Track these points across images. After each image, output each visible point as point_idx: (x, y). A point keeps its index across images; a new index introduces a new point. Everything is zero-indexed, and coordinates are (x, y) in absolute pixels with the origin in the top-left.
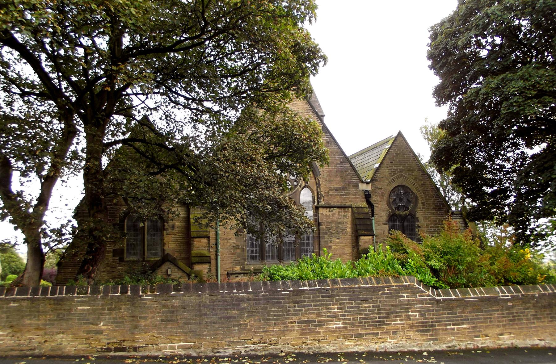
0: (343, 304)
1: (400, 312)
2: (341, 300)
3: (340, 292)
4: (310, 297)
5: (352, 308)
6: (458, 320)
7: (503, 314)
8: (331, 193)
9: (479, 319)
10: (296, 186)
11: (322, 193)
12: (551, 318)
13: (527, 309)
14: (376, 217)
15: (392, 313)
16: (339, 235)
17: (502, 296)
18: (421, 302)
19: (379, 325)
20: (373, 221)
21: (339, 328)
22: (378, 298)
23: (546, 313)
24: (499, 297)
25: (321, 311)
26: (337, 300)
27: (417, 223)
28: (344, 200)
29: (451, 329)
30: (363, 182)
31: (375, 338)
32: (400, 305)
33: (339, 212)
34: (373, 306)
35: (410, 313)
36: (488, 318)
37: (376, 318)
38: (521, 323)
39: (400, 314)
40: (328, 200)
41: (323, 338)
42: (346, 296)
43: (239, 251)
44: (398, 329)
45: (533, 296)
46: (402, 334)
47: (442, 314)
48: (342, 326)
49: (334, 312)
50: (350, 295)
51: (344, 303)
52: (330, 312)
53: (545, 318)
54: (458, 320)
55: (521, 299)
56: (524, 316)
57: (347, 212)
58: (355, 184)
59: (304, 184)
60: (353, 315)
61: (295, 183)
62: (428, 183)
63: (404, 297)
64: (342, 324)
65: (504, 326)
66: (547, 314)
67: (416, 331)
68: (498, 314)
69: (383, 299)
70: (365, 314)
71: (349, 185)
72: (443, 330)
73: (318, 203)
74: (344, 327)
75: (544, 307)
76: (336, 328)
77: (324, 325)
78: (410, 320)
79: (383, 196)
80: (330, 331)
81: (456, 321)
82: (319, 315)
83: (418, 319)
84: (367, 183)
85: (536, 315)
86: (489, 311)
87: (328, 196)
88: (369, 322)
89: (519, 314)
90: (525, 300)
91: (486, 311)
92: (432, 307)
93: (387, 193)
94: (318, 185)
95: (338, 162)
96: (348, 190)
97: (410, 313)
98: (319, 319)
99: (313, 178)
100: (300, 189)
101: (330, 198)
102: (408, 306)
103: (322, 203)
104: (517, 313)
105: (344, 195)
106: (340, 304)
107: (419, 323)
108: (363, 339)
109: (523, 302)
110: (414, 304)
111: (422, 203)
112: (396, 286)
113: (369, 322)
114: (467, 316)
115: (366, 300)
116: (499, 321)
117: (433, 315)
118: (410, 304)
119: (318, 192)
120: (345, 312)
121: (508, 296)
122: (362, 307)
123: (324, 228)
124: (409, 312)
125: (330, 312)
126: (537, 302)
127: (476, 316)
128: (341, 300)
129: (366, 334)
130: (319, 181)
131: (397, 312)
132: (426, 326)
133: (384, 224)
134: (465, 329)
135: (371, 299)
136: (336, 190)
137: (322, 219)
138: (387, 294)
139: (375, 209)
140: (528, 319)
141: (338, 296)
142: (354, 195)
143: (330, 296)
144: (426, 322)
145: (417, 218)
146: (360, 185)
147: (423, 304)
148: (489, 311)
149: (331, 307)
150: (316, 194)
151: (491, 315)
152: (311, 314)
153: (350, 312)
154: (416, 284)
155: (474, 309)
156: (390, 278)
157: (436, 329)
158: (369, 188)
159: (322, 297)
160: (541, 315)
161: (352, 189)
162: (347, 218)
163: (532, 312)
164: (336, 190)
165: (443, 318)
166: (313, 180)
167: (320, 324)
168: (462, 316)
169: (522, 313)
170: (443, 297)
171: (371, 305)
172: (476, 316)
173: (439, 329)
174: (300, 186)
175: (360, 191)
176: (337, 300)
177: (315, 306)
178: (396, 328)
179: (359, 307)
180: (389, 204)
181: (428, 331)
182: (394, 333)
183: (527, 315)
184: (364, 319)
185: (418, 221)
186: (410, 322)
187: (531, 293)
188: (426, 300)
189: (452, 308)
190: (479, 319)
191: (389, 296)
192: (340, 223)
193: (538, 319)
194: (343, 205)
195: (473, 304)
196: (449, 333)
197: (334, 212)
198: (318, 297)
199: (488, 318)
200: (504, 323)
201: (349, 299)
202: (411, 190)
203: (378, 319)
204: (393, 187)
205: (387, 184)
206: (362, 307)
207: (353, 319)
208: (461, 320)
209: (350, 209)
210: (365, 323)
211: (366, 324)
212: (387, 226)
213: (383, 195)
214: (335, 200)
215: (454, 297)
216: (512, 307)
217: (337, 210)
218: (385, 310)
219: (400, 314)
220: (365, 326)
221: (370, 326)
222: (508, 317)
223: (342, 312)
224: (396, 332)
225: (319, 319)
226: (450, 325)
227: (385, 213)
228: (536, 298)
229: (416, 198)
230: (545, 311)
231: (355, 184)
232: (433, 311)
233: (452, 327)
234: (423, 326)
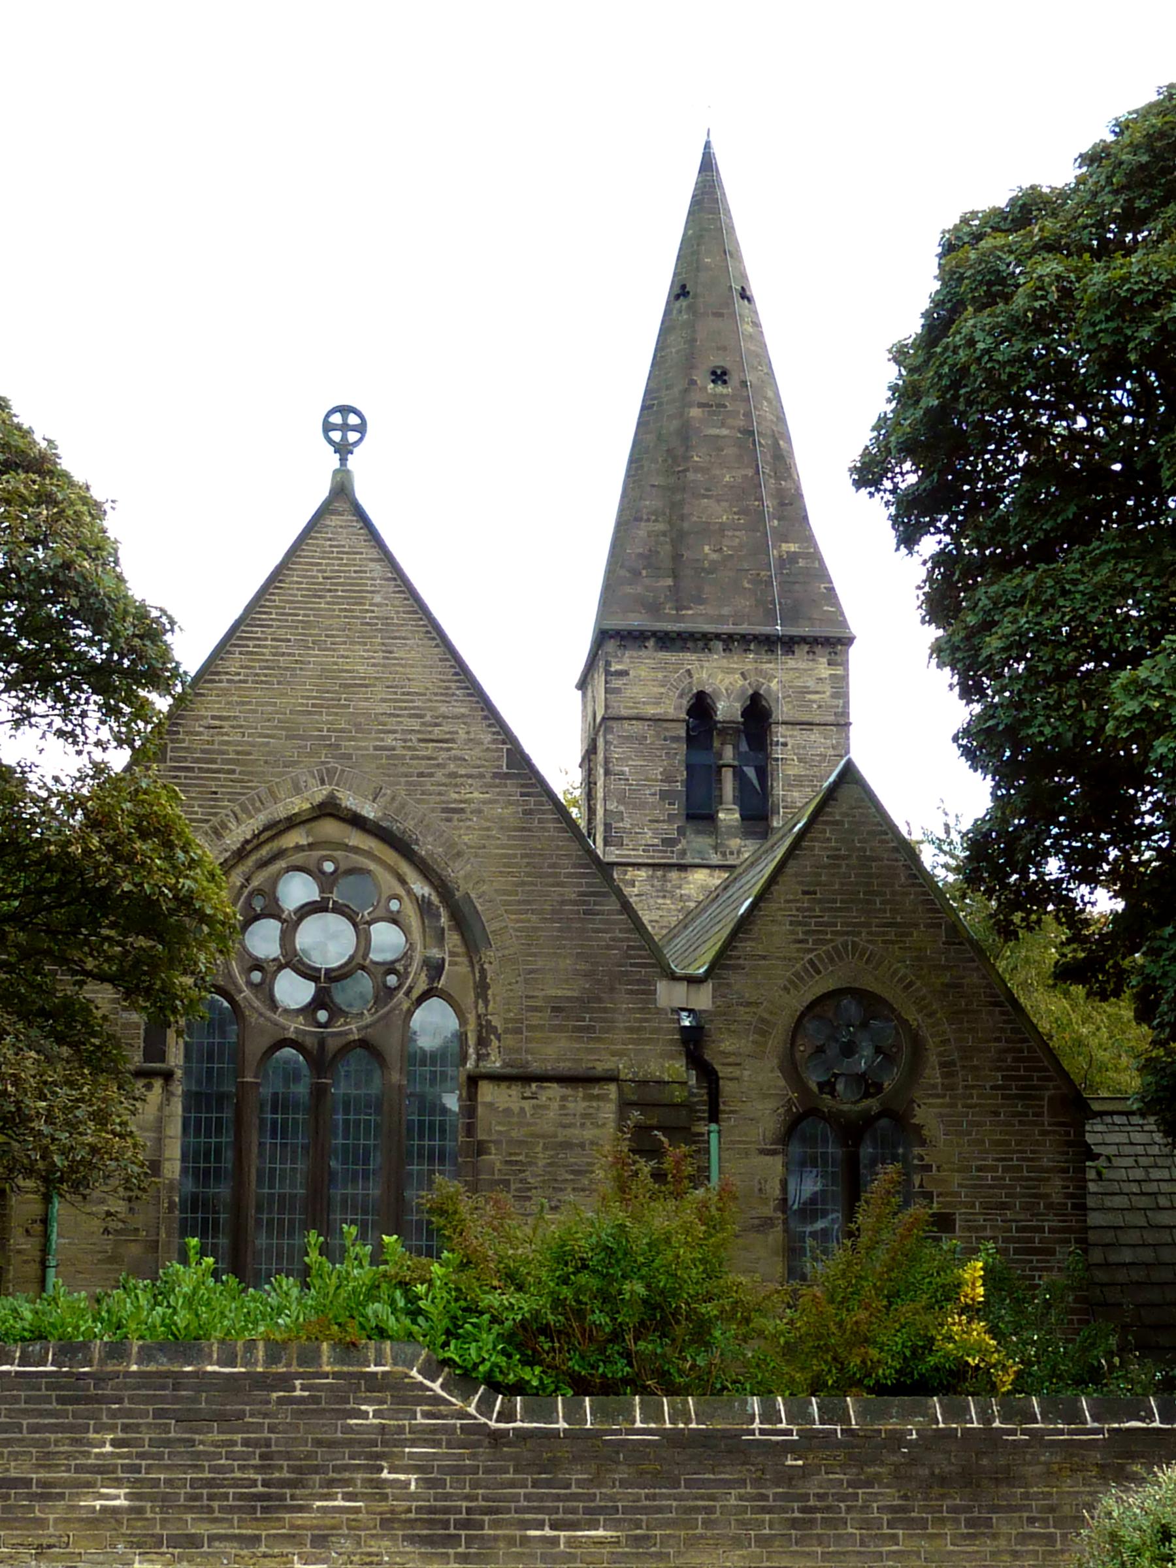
0: (136, 1428)
1: (346, 1468)
2: (129, 1413)
3: (126, 1387)
4: (16, 1399)
5: (168, 1443)
6: (574, 1511)
7: (764, 1497)
8: (535, 1019)
9: (659, 1510)
10: (391, 992)
11: (496, 1022)
12: (970, 1523)
13: (869, 1483)
14: (729, 1122)
15: (316, 1470)
16: (560, 1196)
17: (762, 1432)
18: (428, 1436)
19: (265, 1509)
20: (714, 1137)
21: (115, 1510)
22: (266, 1415)
23: (947, 1503)
24: (752, 1432)
25: (53, 1449)
26: (113, 1415)
27: (917, 1150)
28: (590, 1051)
29: (543, 1539)
30: (674, 977)
31: (244, 1552)
32: (349, 1443)
33: (564, 1098)
34: (246, 1443)
35: (385, 1475)
36: (697, 1510)
37: (254, 1483)
38: (839, 1537)
39: (347, 1475)
40: (518, 1051)
41: (52, 1541)
42: (148, 1400)
43: (135, 1250)
44: (333, 1528)
45: (897, 1439)
46: (349, 1545)
47: (512, 1484)
48: (126, 1503)
49: (98, 1456)
50: (163, 1399)
51: (138, 1425)
52: (87, 1455)
53: (942, 1521)
54: (574, 1511)
55: (840, 1445)
56: (849, 1509)
57: (598, 1098)
58: (639, 982)
59: (422, 986)
60: (168, 1468)
61: (392, 980)
62: (975, 978)
63: (364, 1415)
64: (127, 1497)
65: (762, 1541)
66: (954, 1509)
67: (405, 1538)
68: (741, 1498)
69: (285, 1417)
70: (212, 1469)
71: (612, 990)
72: (511, 1541)
73: (480, 1057)
74: (131, 1510)
75: (943, 1481)
76: (104, 1509)
77: (61, 1496)
78: (384, 1497)
79: (763, 1033)
80: (81, 1520)
81: (567, 1511)
82: (46, 1460)
83: (413, 1497)
84: (692, 980)
85: (903, 1509)
86: (703, 1484)
87: (518, 1031)
88: (225, 1496)
89: (830, 1501)
90: (860, 1451)
91: (689, 1484)
92: (473, 1456)
93: (784, 1022)
94: (482, 989)
95: (571, 893)
96: (605, 1010)
97: (385, 1475)
98: (43, 1475)
99: (463, 960)
100: (405, 1006)
101: (529, 1040)
102: (379, 1448)
103: (495, 1063)
104: (819, 1497)
105: (588, 1029)
106: (126, 1428)
107: (419, 1509)
108: (201, 1555)
109: (850, 1457)
110: (403, 1443)
111: (943, 1065)
112: (336, 1375)
113: (225, 1496)
114: (612, 1498)
115: (222, 1418)
116: (742, 1524)
117: (475, 1485)
118: (385, 1443)
119: (479, 1017)
120: (141, 1456)
121: (788, 1432)
122: (202, 1442)
123: (498, 1165)
124: (381, 1469)
125: (87, 1455)
126: (913, 1461)
127: (647, 1497)
128: (129, 1413)
129: (212, 1538)
130: (483, 971)
131: (336, 1469)
132: (445, 1524)
133: (763, 1152)
134: (600, 1542)
135: (240, 1415)
136: (555, 1009)
137: (489, 1127)
138: (301, 1401)
139: (727, 1087)
140: (866, 1524)
141: (119, 1400)
142: (631, 1030)
143: (89, 1400)
144: (447, 1510)
145: (918, 1128)
146: (662, 987)
147: (437, 1444)
148: (703, 1484)
149: (91, 1435)
150: (472, 1026)
151: (712, 1498)
152: (15, 1456)
153: (160, 1456)
154: (414, 1373)
155: (642, 1473)
156: (325, 1346)
157: (482, 1537)
158: (703, 999)
159: (61, 1400)
160: (923, 1509)
161: (624, 1004)
162: (600, 1123)
163: (890, 1496)
164: (555, 1009)
165: (515, 1498)
166: (464, 969)
167: (47, 1493)
168: (592, 1497)
169: (843, 1498)
170: (518, 1424)
171: (238, 1437)
172: (647, 1497)
173: (496, 1538)
174: (407, 993)
175: (659, 1011)
176: (113, 1415)
177: (34, 1429)
178: (328, 1522)
179: (192, 1442)
180: (791, 1069)
181: (453, 1540)
182: (321, 1541)
183: (865, 1508)
184: (209, 1483)
185: (923, 1143)
186: (383, 1506)
187: (892, 1424)
188: (445, 1429)
189: (553, 1465)
190: (659, 1510)
191: (308, 1409)
192: (567, 1145)
193: (911, 1523)
194: (581, 1069)
195: (637, 1452)
196: (532, 1556)
197: (543, 1098)
198: (47, 1400)
199: (697, 1510)
200: (767, 1531)
201: (158, 1414)
202: (893, 1010)
203: (261, 1489)
204: (810, 997)
205: (781, 982)
206: (202, 1442)
207: (169, 1482)
208: (587, 1511)
209: (612, 1089)
210: (211, 1497)
211: (215, 1504)
212: (777, 1163)
213: (763, 1030)
214: (551, 1051)
215: (562, 1425)
216: (804, 1473)
217: (554, 1090)
218: (288, 1456)
219: (347, 1475)
220: (210, 1510)
221: (231, 1509)
222: (784, 1510)
223: (128, 1456)
224: (325, 1537)
225: (43, 1475)
226: (540, 1525)
227: (770, 1104)
228: (911, 1444)
229: (917, 1046)
230: (943, 1497)
231: (639, 982)
232: (475, 1470)
233: (548, 1532)
234: (431, 1523)
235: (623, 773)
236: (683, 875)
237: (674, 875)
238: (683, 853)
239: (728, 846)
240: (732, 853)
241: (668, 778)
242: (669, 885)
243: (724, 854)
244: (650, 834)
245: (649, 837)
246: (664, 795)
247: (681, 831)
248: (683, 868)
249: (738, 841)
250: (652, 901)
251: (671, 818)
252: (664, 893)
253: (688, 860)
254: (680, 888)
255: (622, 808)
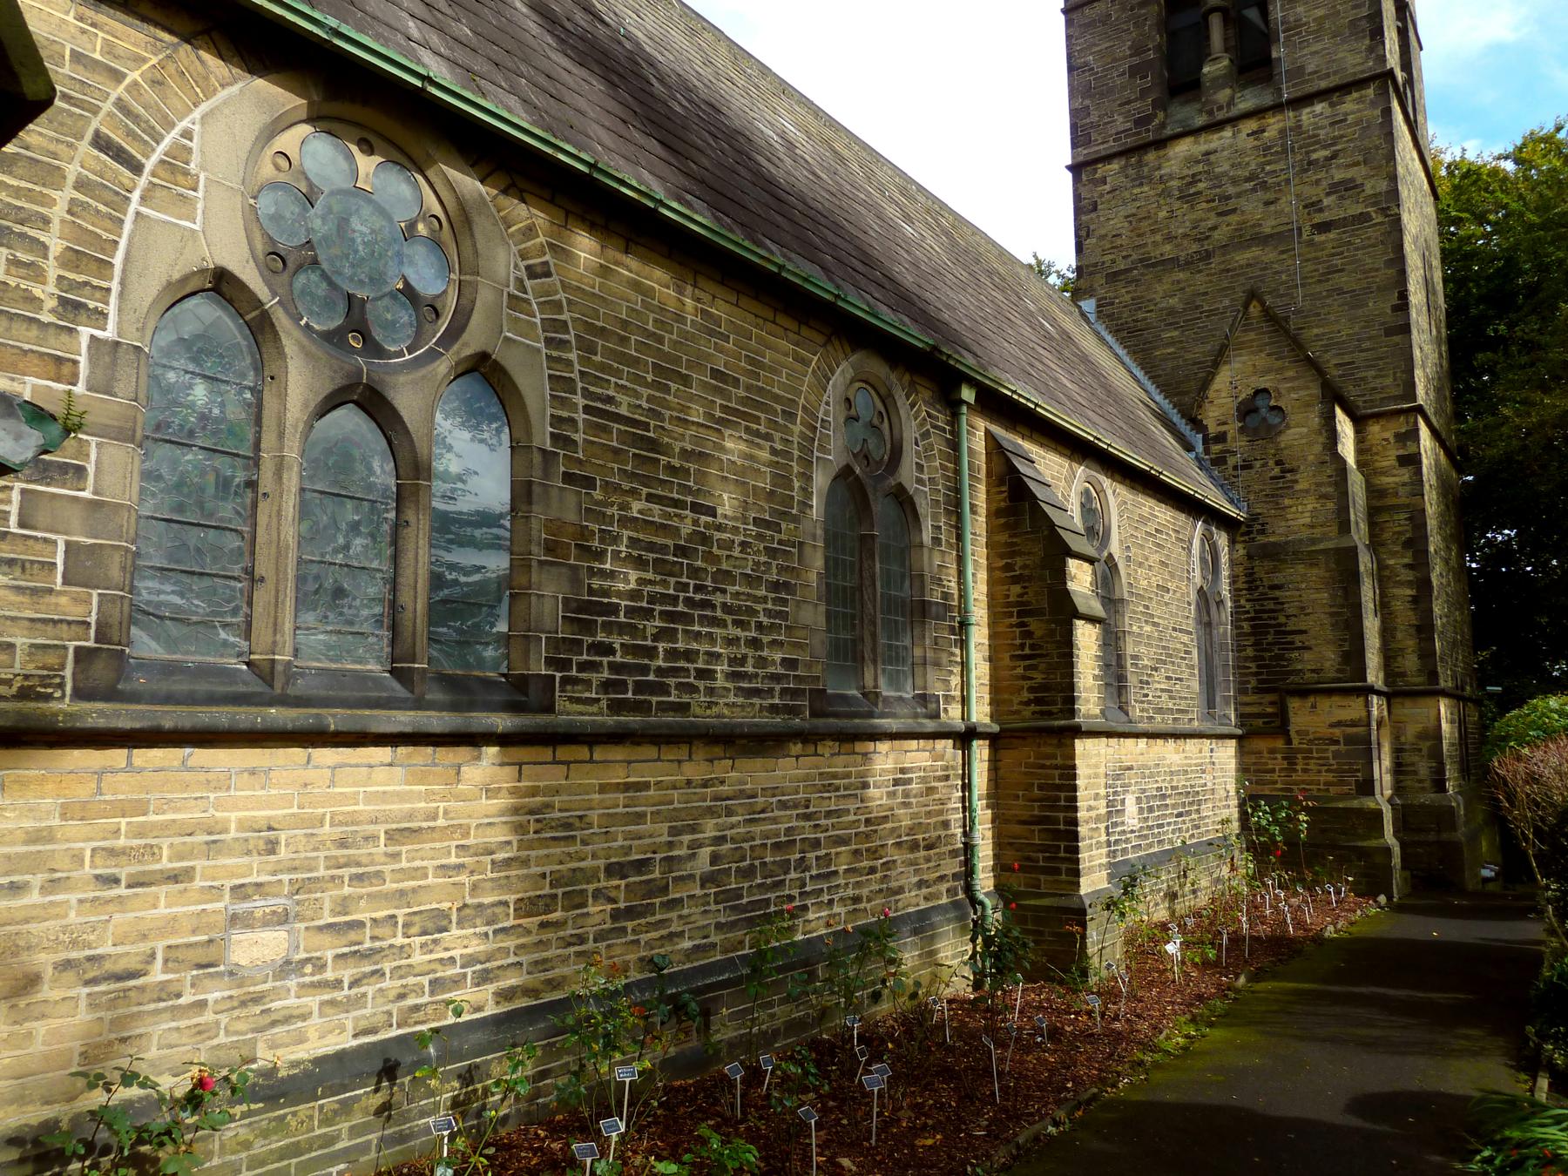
235: (1086, 64)
236: (1162, 153)
237: (1151, 157)
238: (1163, 125)
239: (1215, 102)
240: (1220, 108)
241: (1137, 50)
242: (1146, 169)
243: (1210, 113)
244: (1121, 119)
245: (1120, 123)
246: (1134, 71)
247: (1160, 105)
248: (1161, 143)
249: (1228, 91)
250: (1127, 194)
251: (1144, 93)
252: (1140, 180)
253: (1168, 132)
254: (1159, 168)
255: (1087, 102)
